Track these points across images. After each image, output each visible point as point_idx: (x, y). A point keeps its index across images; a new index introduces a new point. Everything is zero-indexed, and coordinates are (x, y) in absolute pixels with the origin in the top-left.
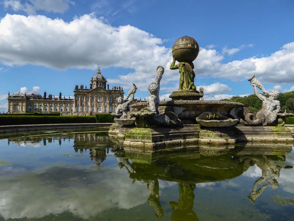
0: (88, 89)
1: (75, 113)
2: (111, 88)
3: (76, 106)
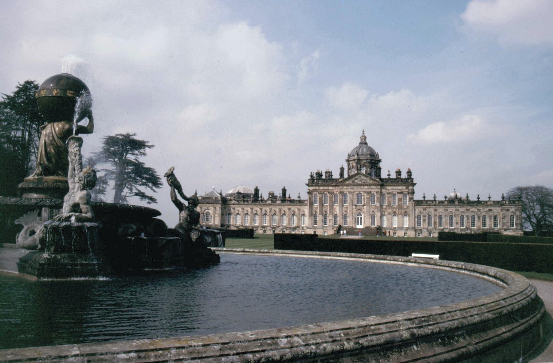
1: (308, 228)
3: (313, 215)
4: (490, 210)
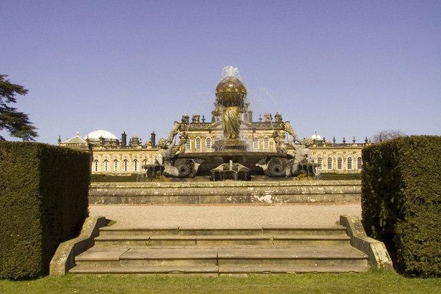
0: (209, 123)
2: (255, 119)
4: (354, 152)
